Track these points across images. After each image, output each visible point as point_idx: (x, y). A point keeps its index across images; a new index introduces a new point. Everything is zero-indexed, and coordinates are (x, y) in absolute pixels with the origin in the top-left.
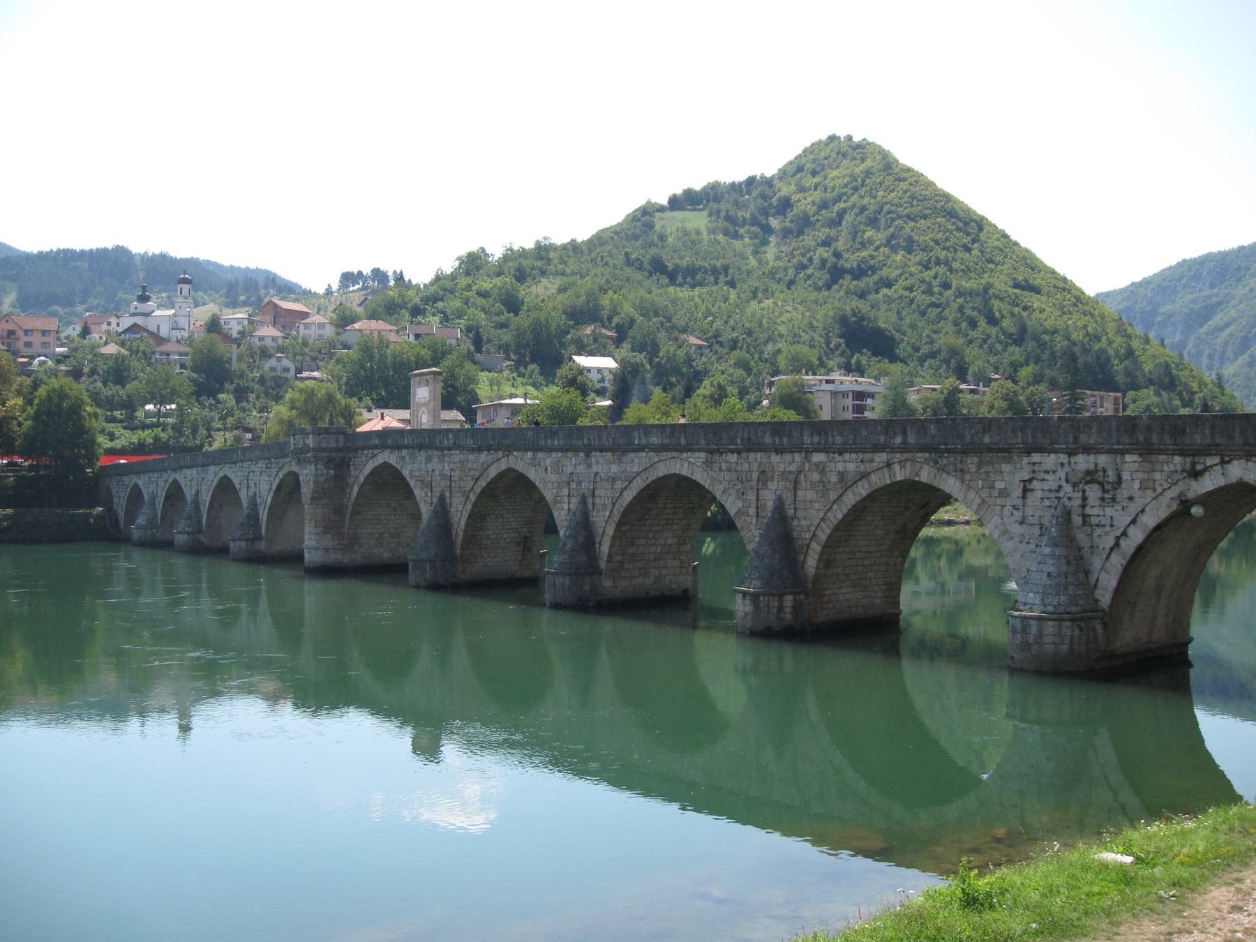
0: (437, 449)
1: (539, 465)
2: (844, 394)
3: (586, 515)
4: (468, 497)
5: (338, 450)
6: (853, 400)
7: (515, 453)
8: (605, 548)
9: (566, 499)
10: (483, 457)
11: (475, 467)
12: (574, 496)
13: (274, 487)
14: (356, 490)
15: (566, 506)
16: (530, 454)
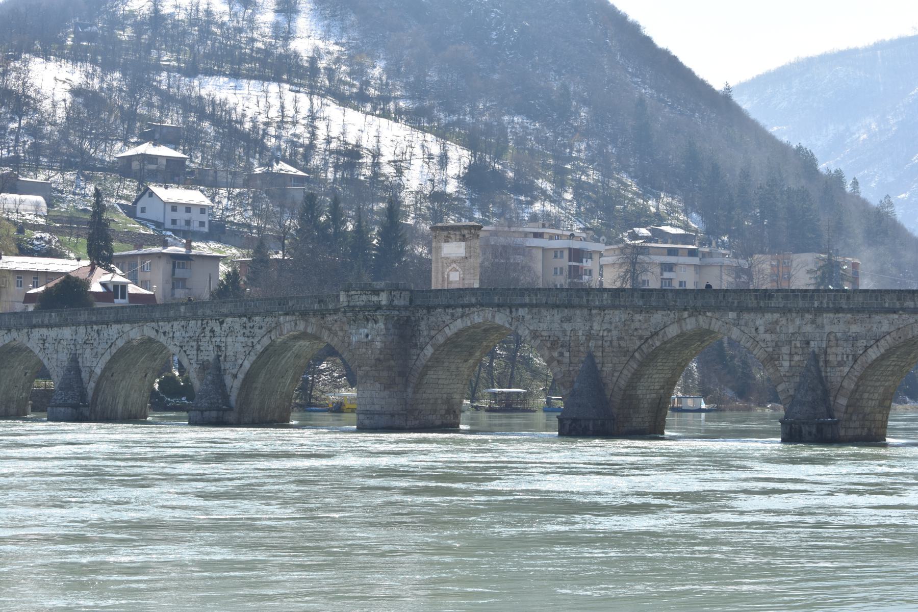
0: (581, 307)
1: (746, 325)
2: (557, 253)
3: (819, 371)
4: (632, 357)
5: (406, 308)
6: (570, 261)
7: (709, 314)
8: (843, 401)
9: (786, 357)
10: (658, 317)
11: (645, 326)
13: (259, 348)
14: (429, 351)
15: (786, 364)
16: (732, 315)
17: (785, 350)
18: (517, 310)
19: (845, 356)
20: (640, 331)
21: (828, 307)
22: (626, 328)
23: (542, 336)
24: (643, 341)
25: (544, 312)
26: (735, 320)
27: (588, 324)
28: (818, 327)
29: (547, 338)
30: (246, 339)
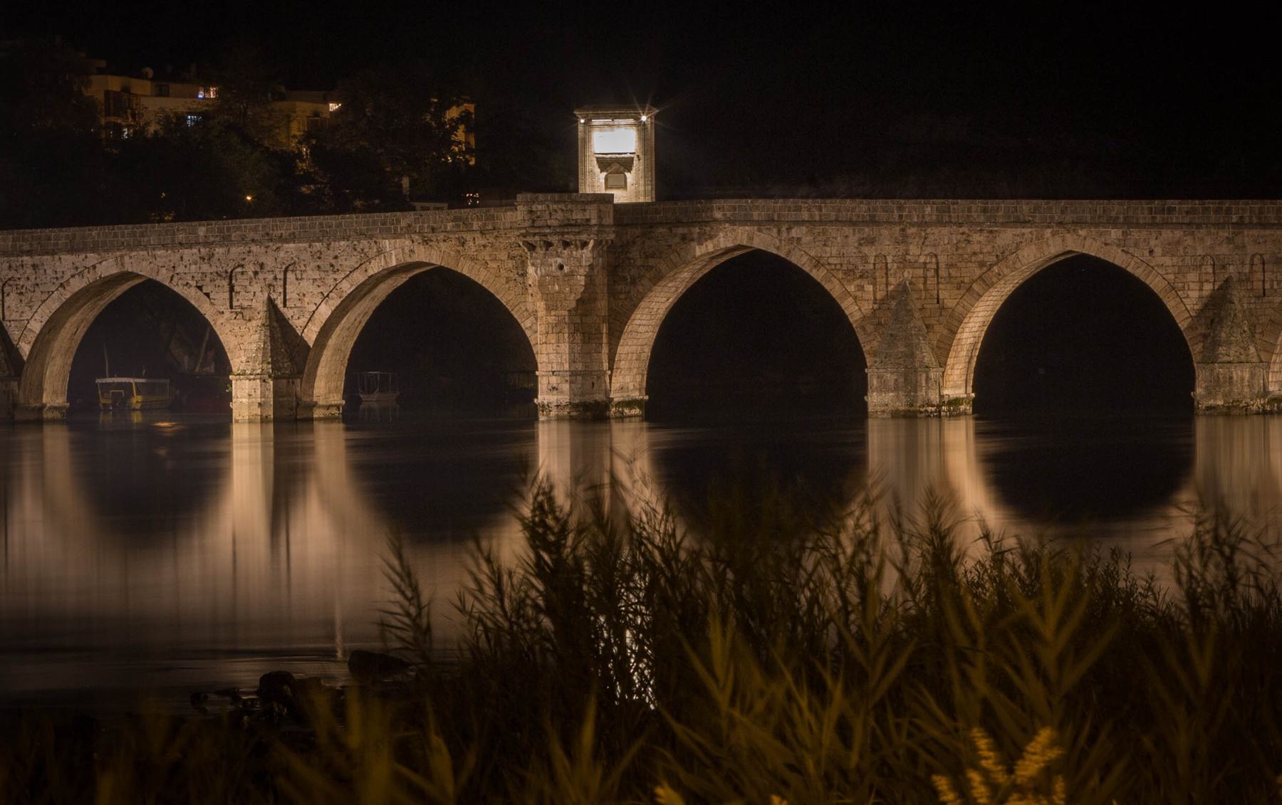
1: (1136, 245)
7: (1082, 233)
11: (989, 248)
12: (1207, 281)
15: (1194, 294)
16: (1115, 234)
17: (1192, 276)
18: (789, 229)
19: (1275, 283)
20: (981, 256)
21: (1251, 223)
22: (960, 251)
23: (829, 264)
24: (985, 269)
25: (832, 231)
26: (1119, 240)
27: (902, 247)
28: (1237, 247)
29: (838, 267)
30: (323, 275)
